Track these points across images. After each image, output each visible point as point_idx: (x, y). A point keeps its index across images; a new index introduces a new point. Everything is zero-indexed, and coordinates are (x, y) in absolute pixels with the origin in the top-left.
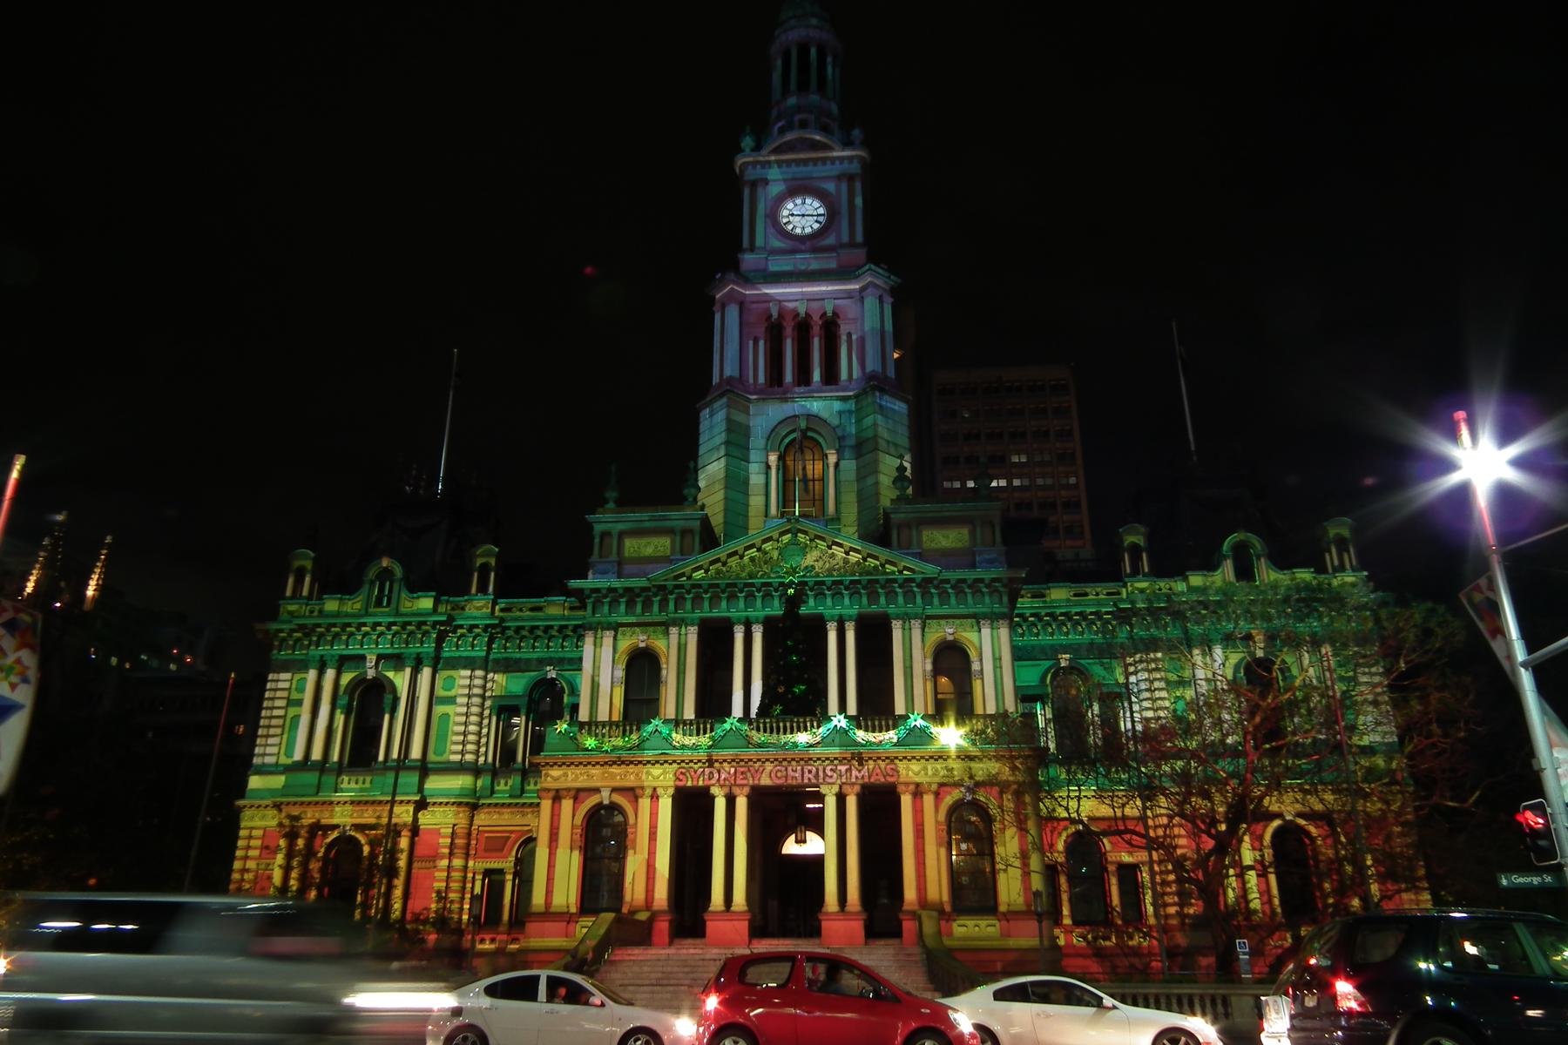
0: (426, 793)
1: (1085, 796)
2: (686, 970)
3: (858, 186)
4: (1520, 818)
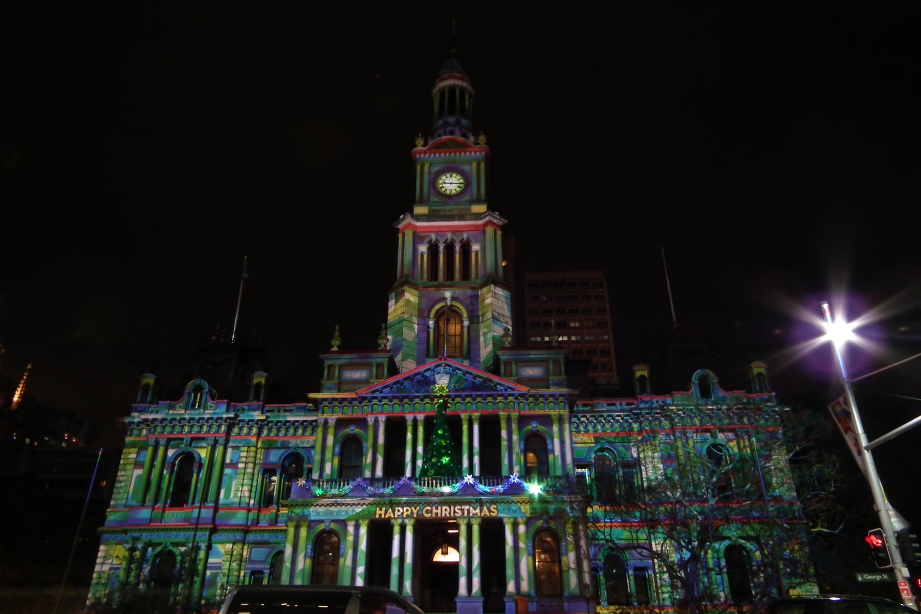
1: (615, 526)
3: (482, 165)
4: (868, 540)
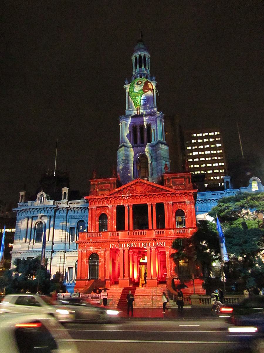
0: (53, 249)
2: (111, 293)
